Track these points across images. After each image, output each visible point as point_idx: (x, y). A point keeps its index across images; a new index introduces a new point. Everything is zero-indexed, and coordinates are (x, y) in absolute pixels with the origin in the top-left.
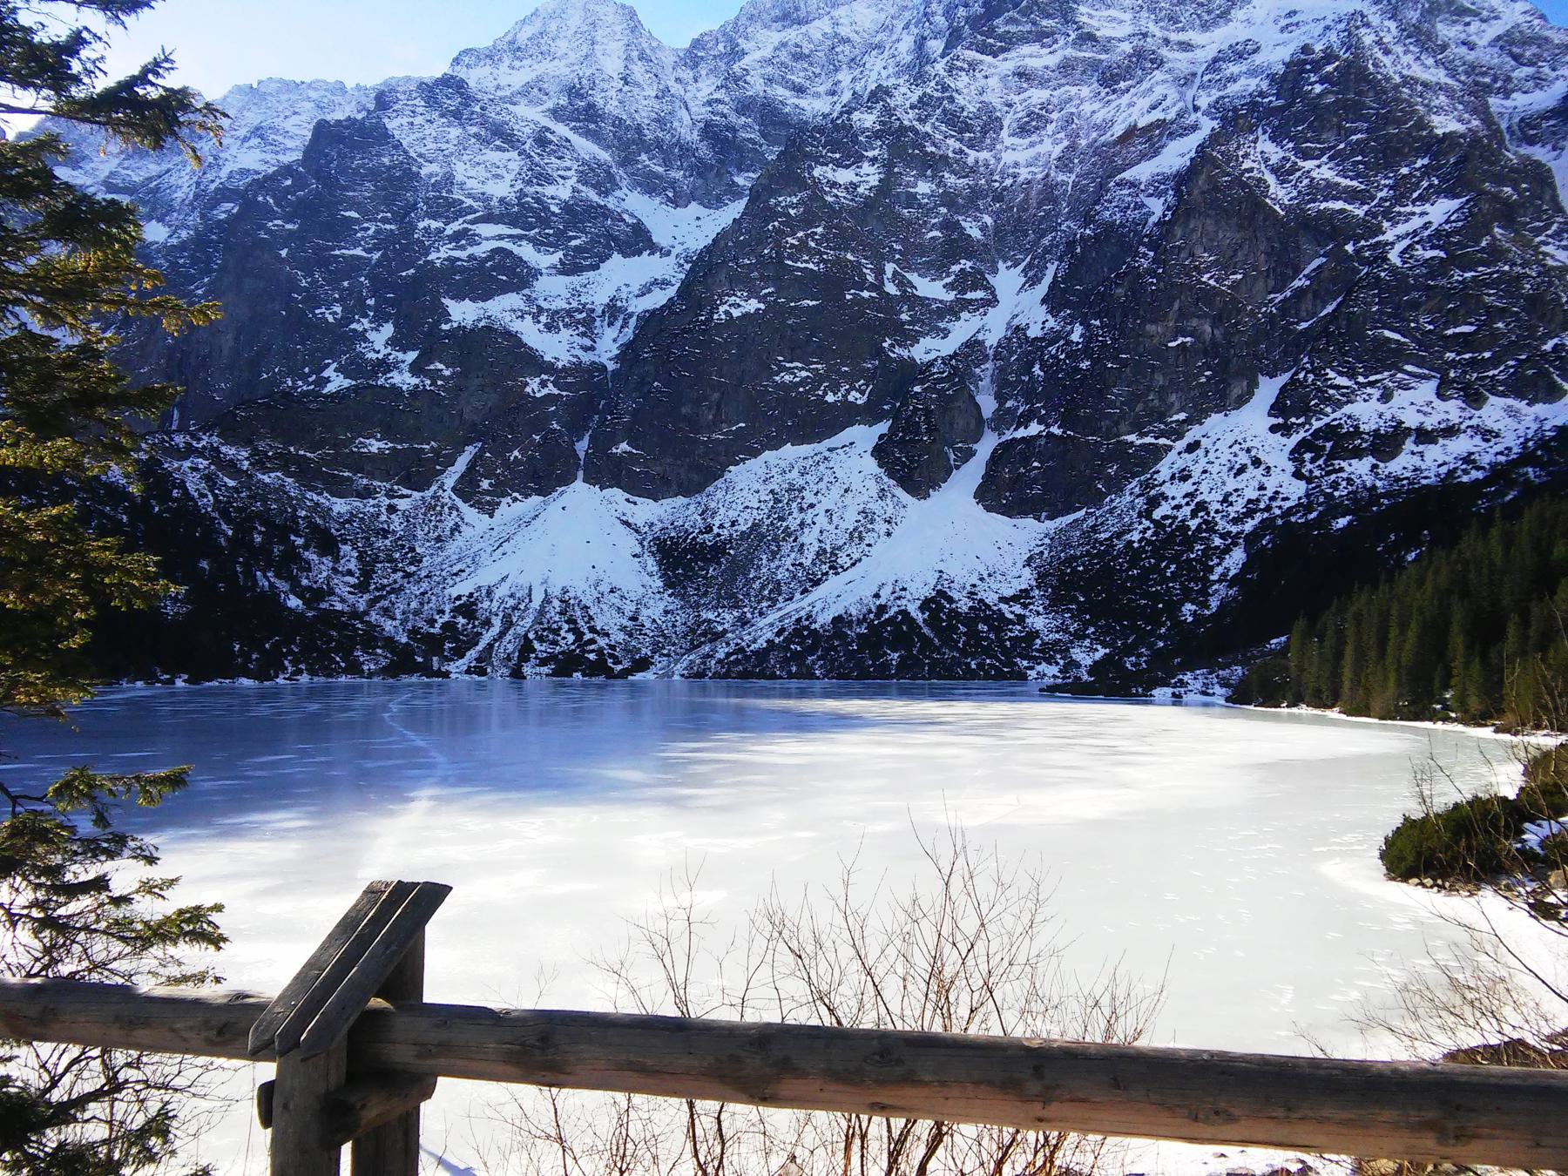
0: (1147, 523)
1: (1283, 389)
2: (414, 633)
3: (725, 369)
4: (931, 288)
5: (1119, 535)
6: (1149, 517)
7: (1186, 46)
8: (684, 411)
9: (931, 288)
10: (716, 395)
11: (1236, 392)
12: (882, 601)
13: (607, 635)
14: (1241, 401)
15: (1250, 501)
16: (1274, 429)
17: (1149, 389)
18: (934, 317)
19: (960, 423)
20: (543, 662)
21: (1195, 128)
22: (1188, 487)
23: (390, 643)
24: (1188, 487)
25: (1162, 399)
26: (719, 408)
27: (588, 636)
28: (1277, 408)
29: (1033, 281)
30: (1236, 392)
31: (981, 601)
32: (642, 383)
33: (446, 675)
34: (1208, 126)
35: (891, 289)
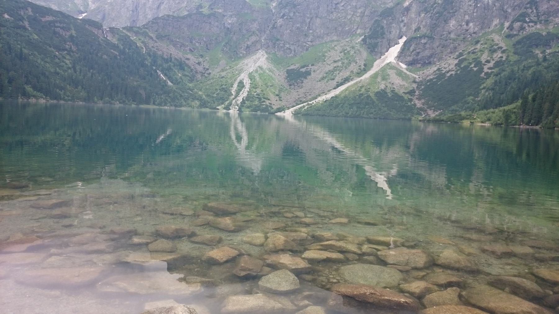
0: (458, 68)
2: (208, 96)
3: (313, 11)
6: (459, 66)
8: (298, 25)
10: (309, 20)
12: (361, 92)
13: (269, 100)
17: (462, 20)
20: (248, 107)
22: (473, 56)
23: (200, 99)
24: (473, 56)
25: (467, 25)
26: (309, 25)
27: (263, 100)
31: (396, 94)
32: (284, 15)
33: (218, 109)
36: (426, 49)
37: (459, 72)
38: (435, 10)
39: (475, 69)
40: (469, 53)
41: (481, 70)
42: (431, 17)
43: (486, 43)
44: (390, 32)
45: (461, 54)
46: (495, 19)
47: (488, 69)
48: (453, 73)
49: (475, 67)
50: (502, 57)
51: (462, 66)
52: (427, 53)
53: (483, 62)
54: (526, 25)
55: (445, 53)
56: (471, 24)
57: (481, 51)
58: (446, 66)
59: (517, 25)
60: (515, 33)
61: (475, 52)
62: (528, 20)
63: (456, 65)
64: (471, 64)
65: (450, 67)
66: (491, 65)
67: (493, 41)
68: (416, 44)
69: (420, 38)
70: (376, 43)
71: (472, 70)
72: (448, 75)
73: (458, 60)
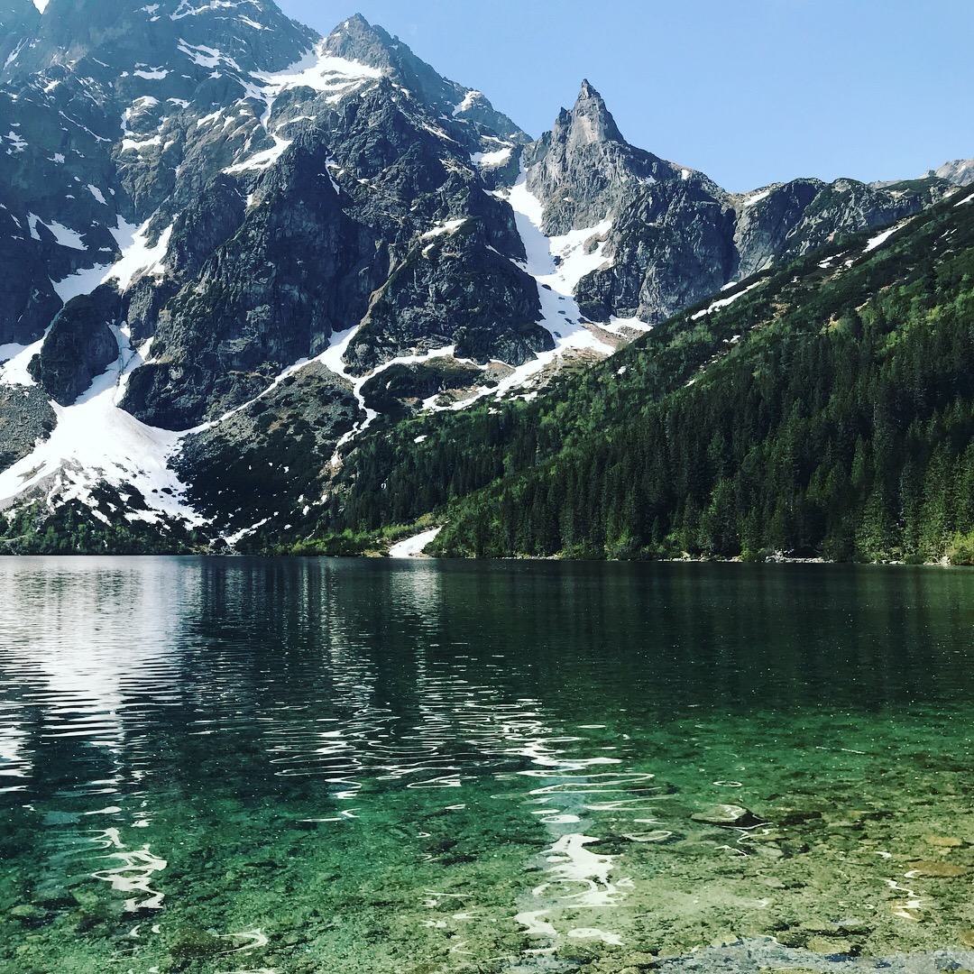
0: (262, 436)
1: (353, 342)
4: (68, 238)
5: (243, 443)
6: (264, 432)
7: (260, 84)
9: (68, 238)
11: (317, 342)
14: (323, 348)
15: (337, 423)
16: (347, 371)
18: (69, 262)
19: (101, 350)
21: (270, 144)
28: (350, 354)
29: (152, 244)
30: (317, 342)
34: (282, 145)
35: (35, 235)
36: (182, 393)
37: (265, 444)
38: (193, 309)
39: (298, 438)
40: (278, 403)
41: (310, 440)
42: (185, 323)
43: (308, 385)
44: (94, 350)
45: (258, 408)
46: (316, 335)
47: (324, 437)
48: (254, 445)
49: (297, 433)
50: (344, 414)
51: (269, 432)
52: (185, 402)
53: (312, 424)
54: (377, 350)
55: (223, 401)
56: (272, 343)
57: (302, 400)
58: (235, 431)
59: (361, 349)
60: (360, 364)
61: (291, 403)
62: (380, 341)
63: (256, 429)
64: (286, 426)
65: (245, 435)
66: (327, 430)
67: (321, 379)
68: (160, 382)
69: (165, 367)
70: (66, 375)
71: (291, 439)
72: (244, 450)
73: (257, 419)
